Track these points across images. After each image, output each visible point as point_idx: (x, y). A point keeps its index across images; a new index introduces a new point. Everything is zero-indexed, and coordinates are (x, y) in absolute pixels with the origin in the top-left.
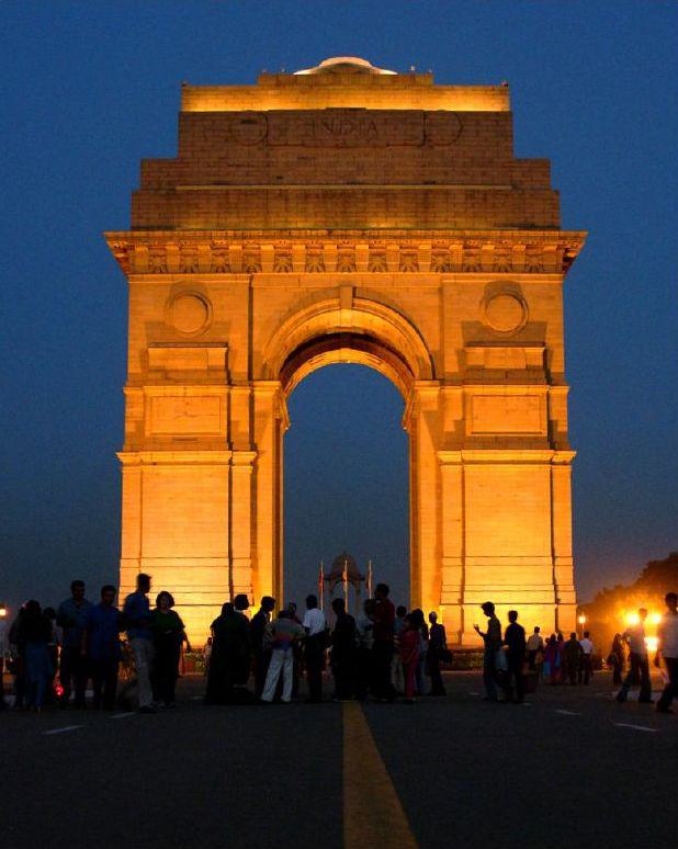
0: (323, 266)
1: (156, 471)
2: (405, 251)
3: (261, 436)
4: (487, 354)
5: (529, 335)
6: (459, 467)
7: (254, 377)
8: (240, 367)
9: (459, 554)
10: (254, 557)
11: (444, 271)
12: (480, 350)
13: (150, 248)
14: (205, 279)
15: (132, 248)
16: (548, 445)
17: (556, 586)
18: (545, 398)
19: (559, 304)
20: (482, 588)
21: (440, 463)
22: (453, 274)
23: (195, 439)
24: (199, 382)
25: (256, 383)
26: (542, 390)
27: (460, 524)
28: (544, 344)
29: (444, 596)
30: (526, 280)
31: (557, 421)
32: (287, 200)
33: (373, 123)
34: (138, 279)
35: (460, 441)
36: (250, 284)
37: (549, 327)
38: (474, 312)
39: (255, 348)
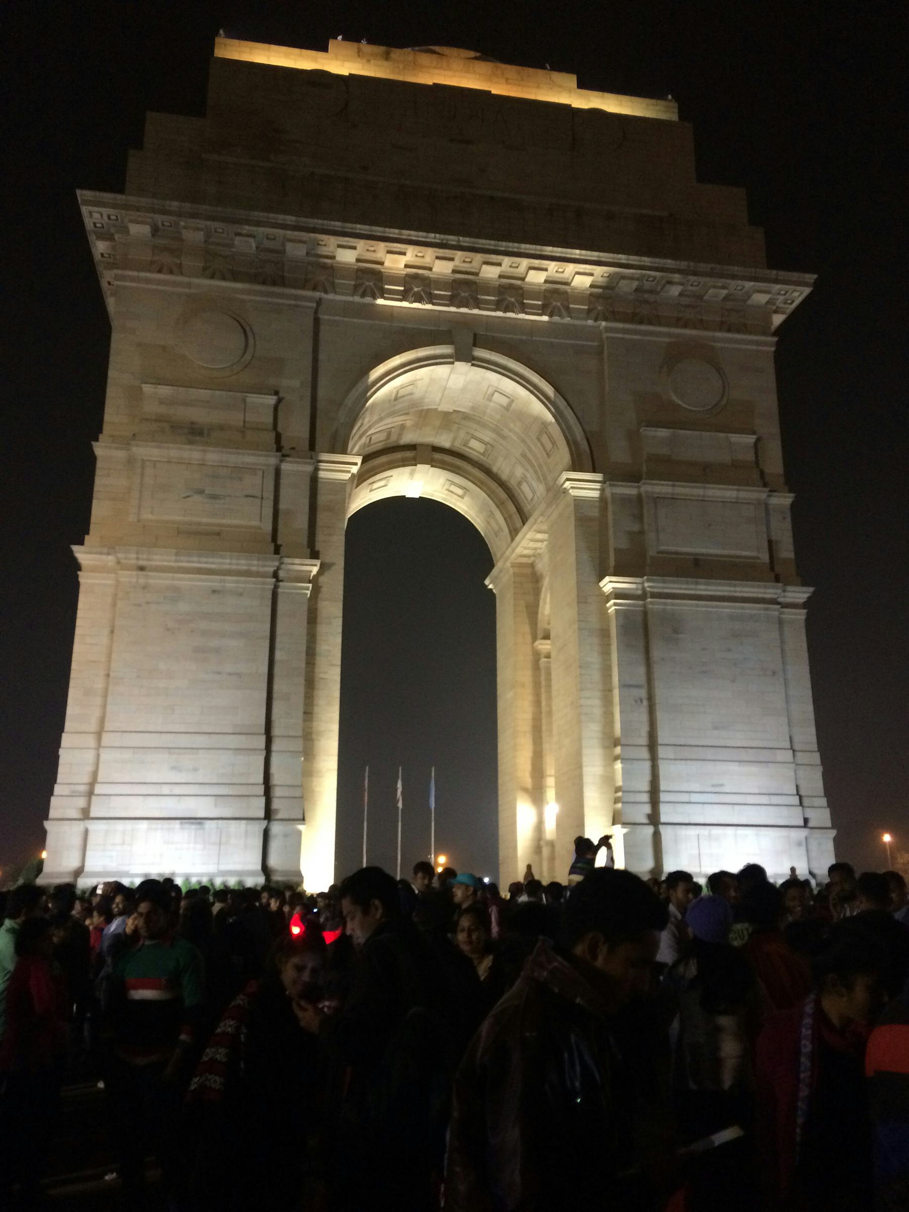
1: (142, 581)
8: (296, 428)
9: (644, 740)
11: (606, 319)
12: (663, 433)
13: (155, 231)
17: (801, 797)
19: (769, 380)
20: (684, 797)
22: (620, 325)
23: (219, 534)
28: (754, 433)
39: (321, 405)
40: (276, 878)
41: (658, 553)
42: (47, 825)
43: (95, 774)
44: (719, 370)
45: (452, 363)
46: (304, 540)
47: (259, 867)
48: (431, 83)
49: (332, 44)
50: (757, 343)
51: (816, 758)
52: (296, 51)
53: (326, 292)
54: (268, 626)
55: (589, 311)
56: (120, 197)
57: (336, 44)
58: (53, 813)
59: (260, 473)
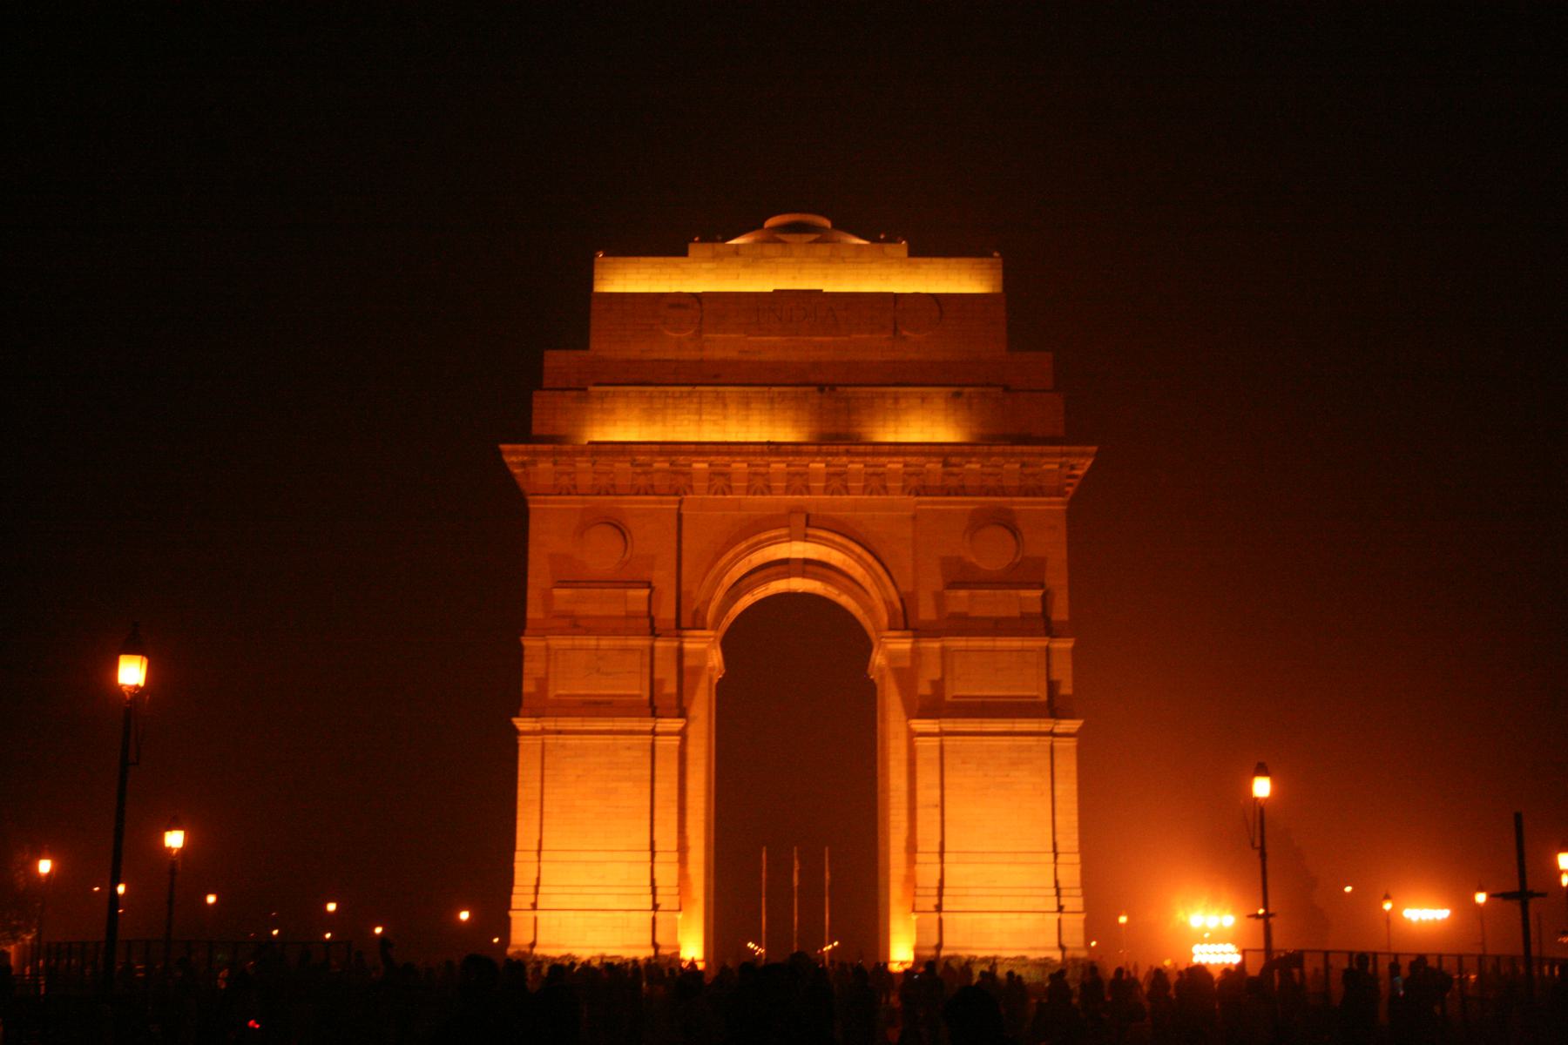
2: (871, 470)
5: (1024, 574)
6: (935, 741)
7: (683, 625)
8: (666, 613)
9: (937, 849)
10: (683, 849)
11: (918, 495)
12: (963, 593)
13: (555, 464)
15: (534, 463)
20: (964, 892)
21: (912, 735)
23: (609, 703)
24: (615, 632)
26: (1039, 643)
27: (938, 811)
28: (1042, 586)
29: (919, 900)
30: (1019, 504)
31: (1058, 682)
34: (540, 502)
35: (933, 707)
39: (684, 588)
40: (662, 951)
42: (512, 914)
43: (538, 879)
44: (1015, 532)
46: (674, 703)
47: (649, 942)
48: (770, 289)
49: (691, 247)
50: (1049, 503)
51: (1076, 858)
52: (661, 259)
54: (648, 772)
55: (903, 488)
56: (530, 447)
58: (514, 906)
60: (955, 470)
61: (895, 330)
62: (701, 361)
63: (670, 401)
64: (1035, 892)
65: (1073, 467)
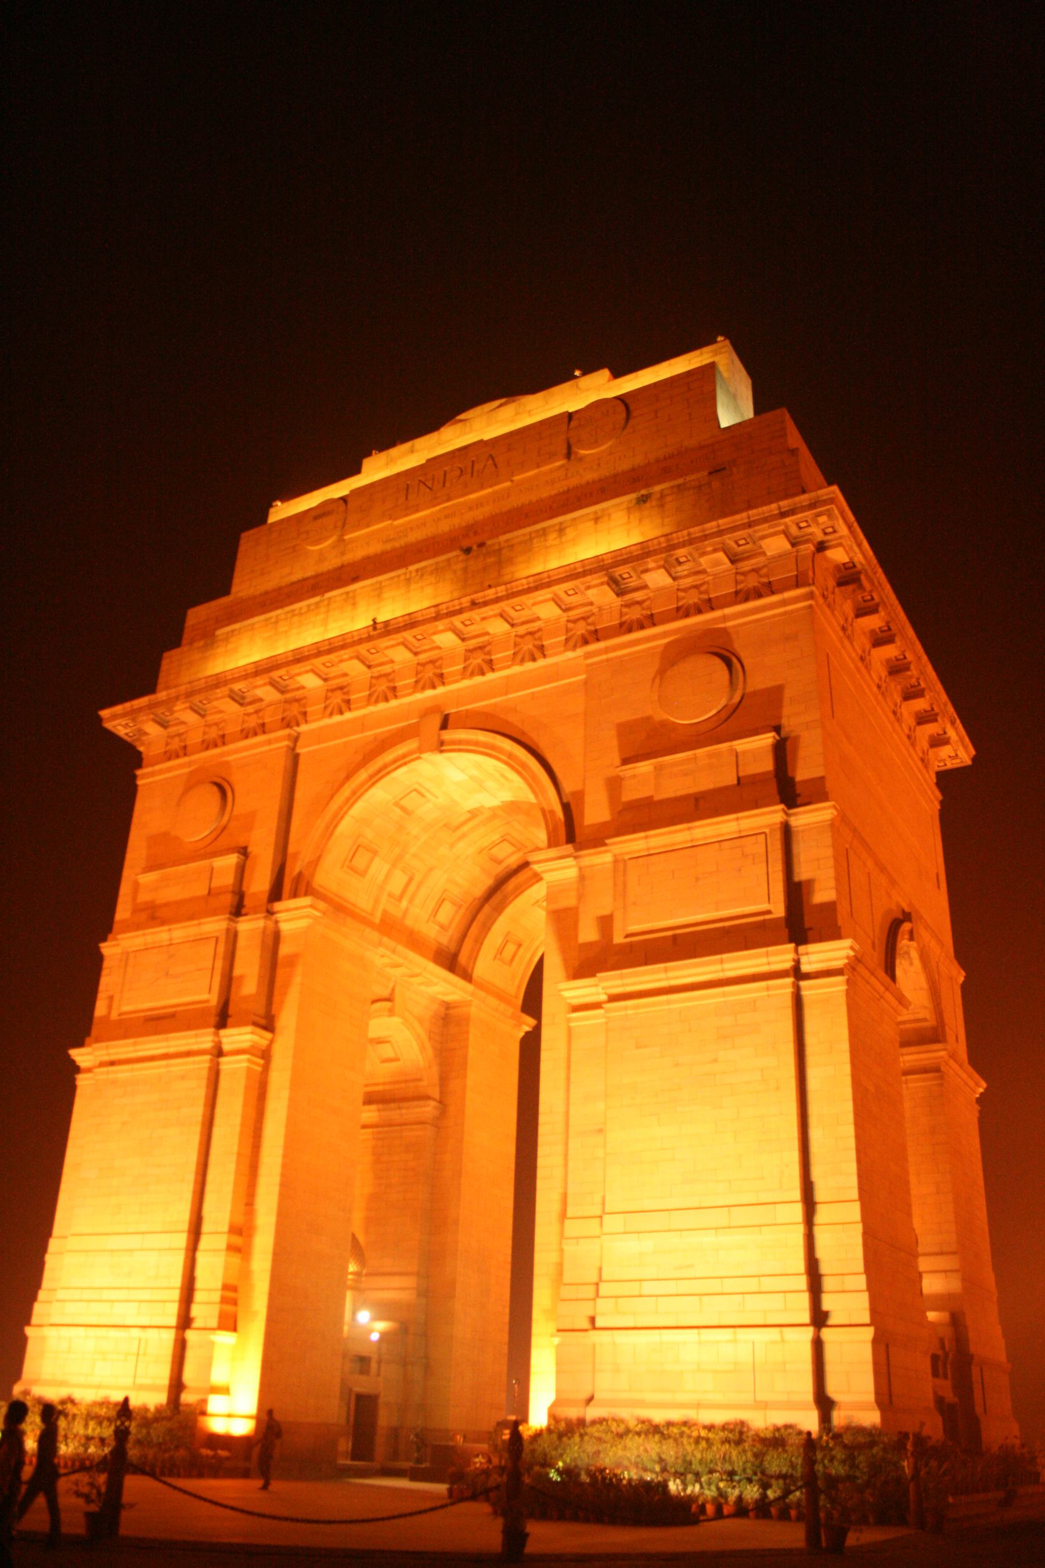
0: (394, 689)
3: (282, 1002)
4: (659, 769)
8: (260, 883)
11: (586, 642)
12: (645, 767)
14: (229, 753)
16: (785, 932)
18: (778, 836)
20: (633, 1288)
22: (602, 645)
23: (173, 1015)
25: (278, 906)
28: (777, 729)
32: (354, 604)
33: (491, 456)
36: (293, 749)
37: (787, 694)
38: (642, 703)
41: (627, 936)
42: (29, 1331)
45: (418, 758)
48: (423, 461)
50: (784, 603)
51: (854, 1212)
53: (298, 725)
54: (198, 1111)
57: (367, 464)
58: (34, 1320)
59: (213, 941)
60: (638, 596)
61: (569, 455)
62: (343, 566)
63: (296, 619)
64: (768, 1284)
65: (821, 547)
